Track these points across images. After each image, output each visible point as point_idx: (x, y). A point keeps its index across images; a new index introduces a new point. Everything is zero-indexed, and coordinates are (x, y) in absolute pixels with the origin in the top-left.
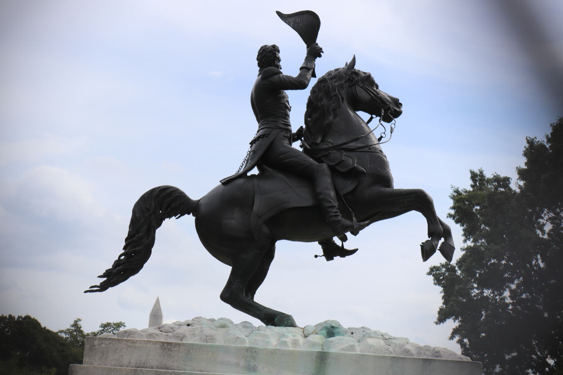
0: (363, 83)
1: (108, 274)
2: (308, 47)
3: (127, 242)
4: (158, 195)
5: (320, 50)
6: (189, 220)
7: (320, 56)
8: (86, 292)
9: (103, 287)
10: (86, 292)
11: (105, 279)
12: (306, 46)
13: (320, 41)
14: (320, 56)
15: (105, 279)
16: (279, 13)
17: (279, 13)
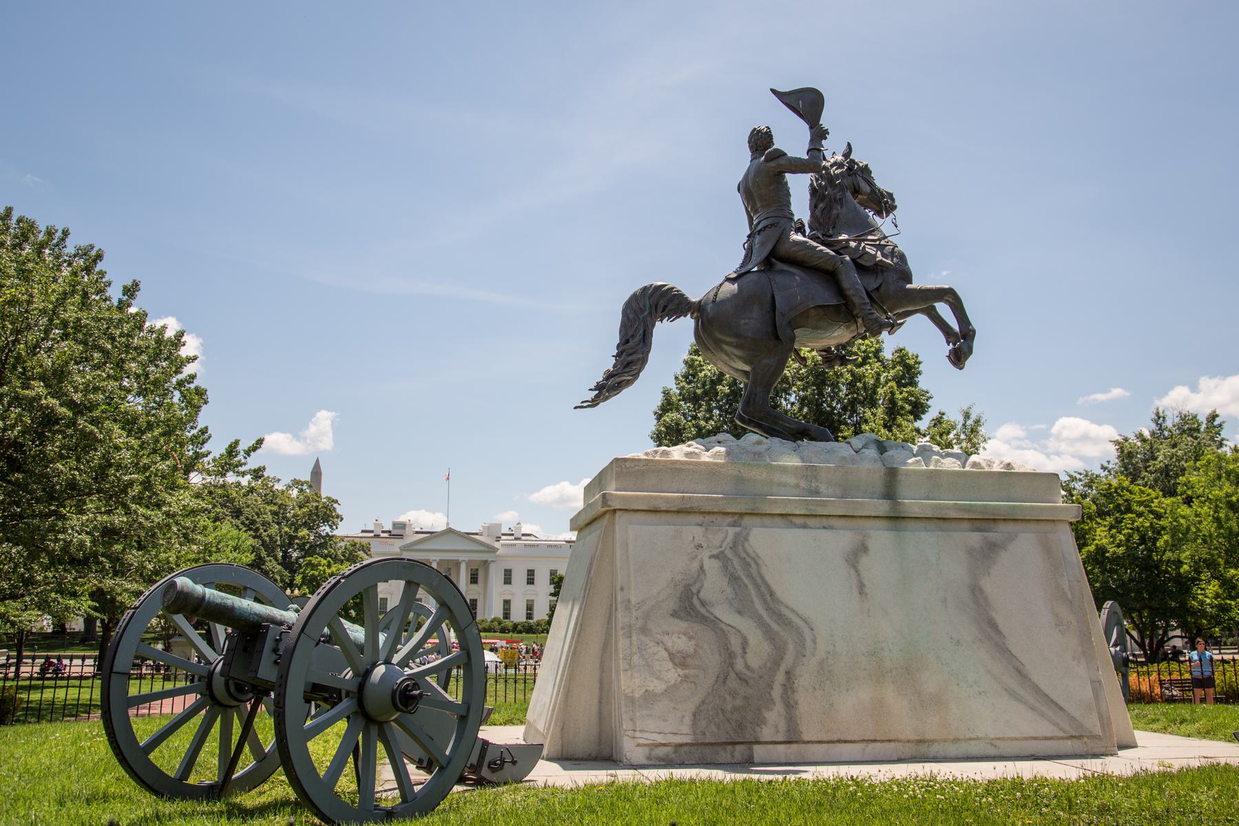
0: (862, 172)
1: (600, 387)
2: (811, 128)
3: (621, 349)
4: (651, 295)
5: (826, 132)
6: (685, 326)
7: (826, 138)
8: (575, 408)
9: (594, 403)
10: (575, 408)
11: (597, 392)
12: (807, 127)
13: (825, 121)
14: (826, 138)
15: (597, 392)
16: (773, 91)
17: (773, 91)
